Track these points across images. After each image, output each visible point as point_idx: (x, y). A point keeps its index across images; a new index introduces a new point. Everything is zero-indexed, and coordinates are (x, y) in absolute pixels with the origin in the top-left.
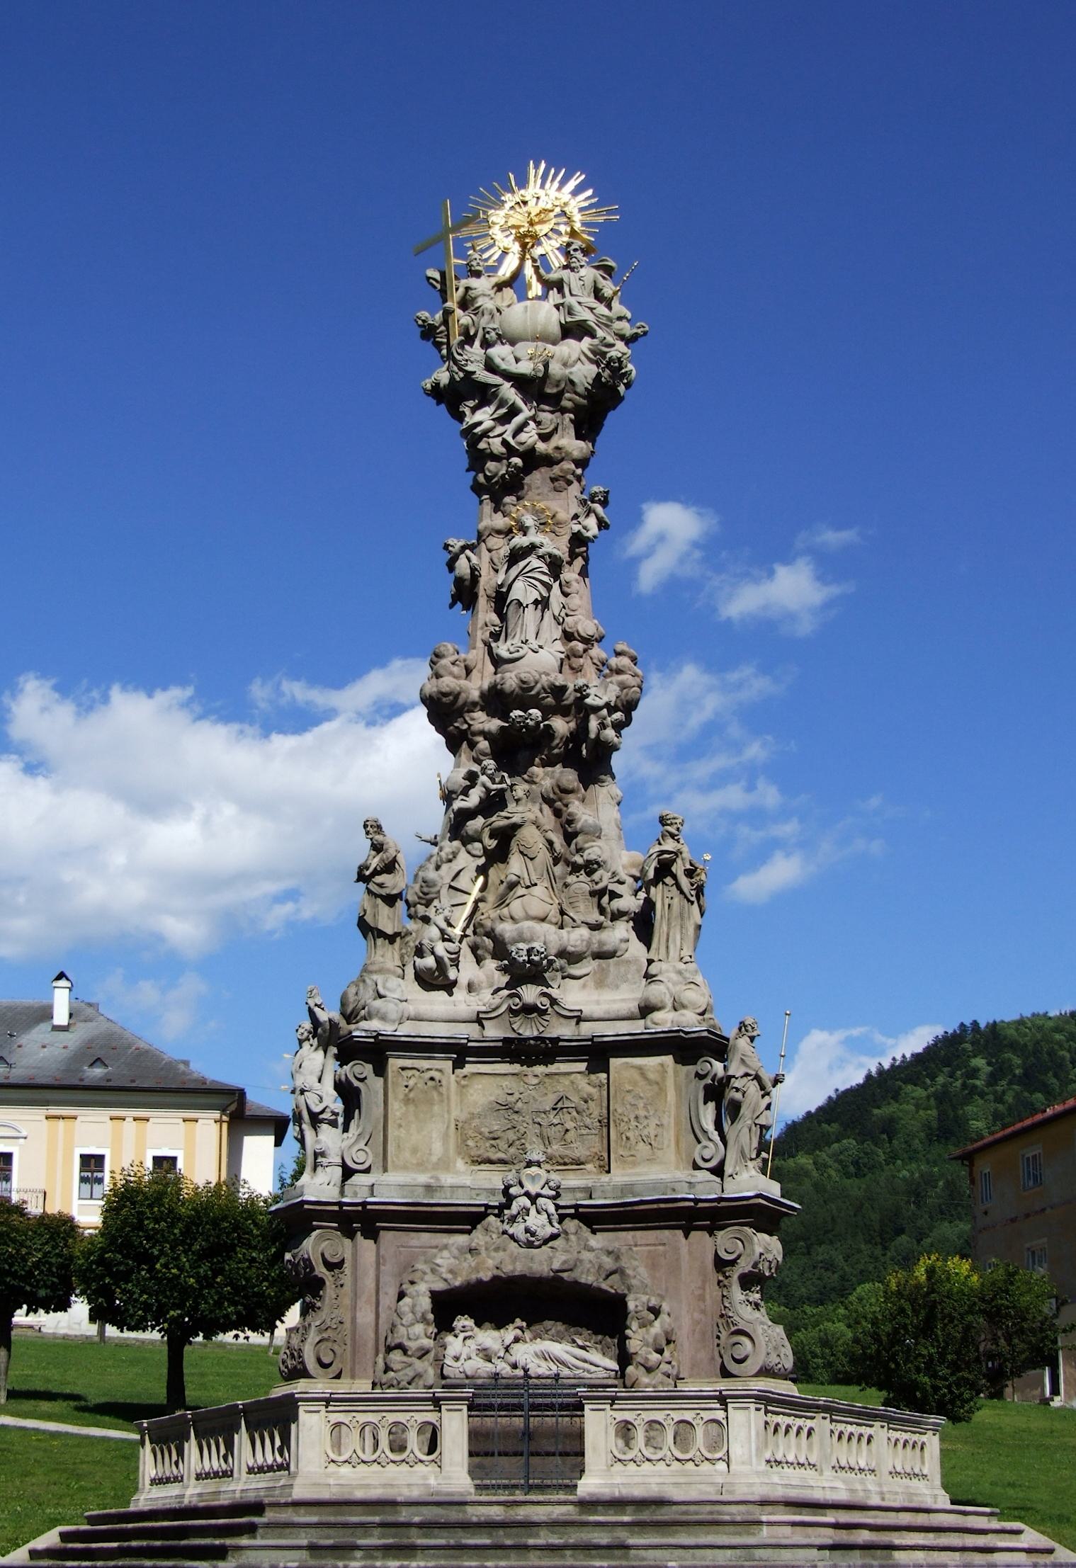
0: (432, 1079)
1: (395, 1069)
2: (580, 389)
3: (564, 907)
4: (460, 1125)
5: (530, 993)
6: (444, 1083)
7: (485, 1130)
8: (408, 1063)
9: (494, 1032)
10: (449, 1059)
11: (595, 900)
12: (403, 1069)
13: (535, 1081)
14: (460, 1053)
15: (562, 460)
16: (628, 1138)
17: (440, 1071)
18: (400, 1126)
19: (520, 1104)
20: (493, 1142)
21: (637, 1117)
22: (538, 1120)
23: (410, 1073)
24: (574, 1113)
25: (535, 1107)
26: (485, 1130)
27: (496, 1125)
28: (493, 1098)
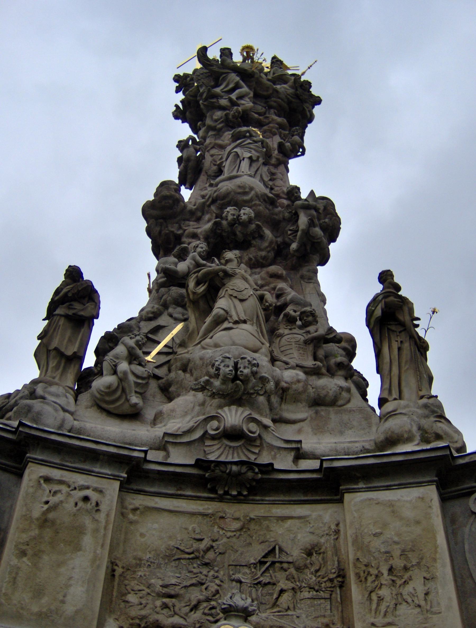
0: (86, 499)
1: (34, 477)
2: (282, 96)
3: (275, 353)
4: (119, 571)
5: (233, 417)
6: (103, 507)
7: (157, 583)
8: (56, 474)
9: (180, 457)
10: (115, 478)
11: (311, 348)
12: (47, 480)
13: (236, 525)
14: (135, 473)
15: (270, 123)
16: (381, 599)
17: (100, 491)
18: (23, 553)
19: (210, 555)
20: (166, 600)
21: (391, 570)
22: (238, 576)
23: (56, 487)
24: (292, 570)
25: (231, 557)
26: (157, 583)
27: (171, 575)
28: (172, 543)
